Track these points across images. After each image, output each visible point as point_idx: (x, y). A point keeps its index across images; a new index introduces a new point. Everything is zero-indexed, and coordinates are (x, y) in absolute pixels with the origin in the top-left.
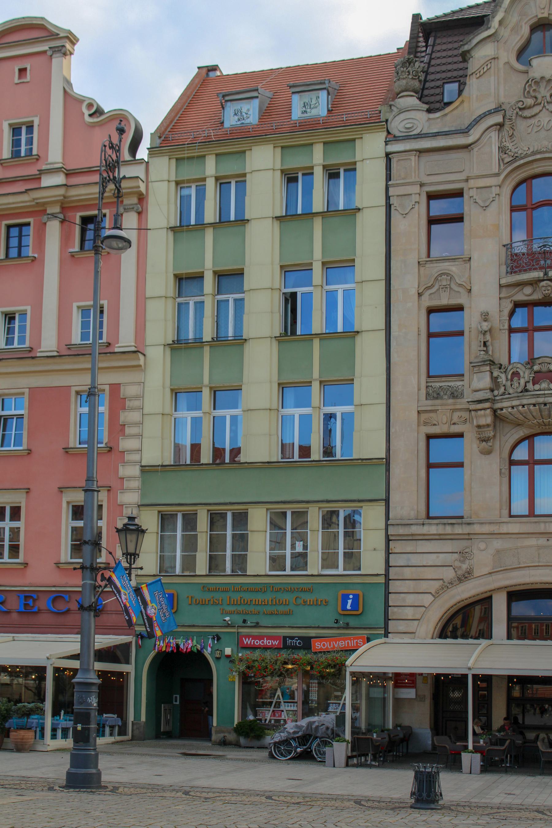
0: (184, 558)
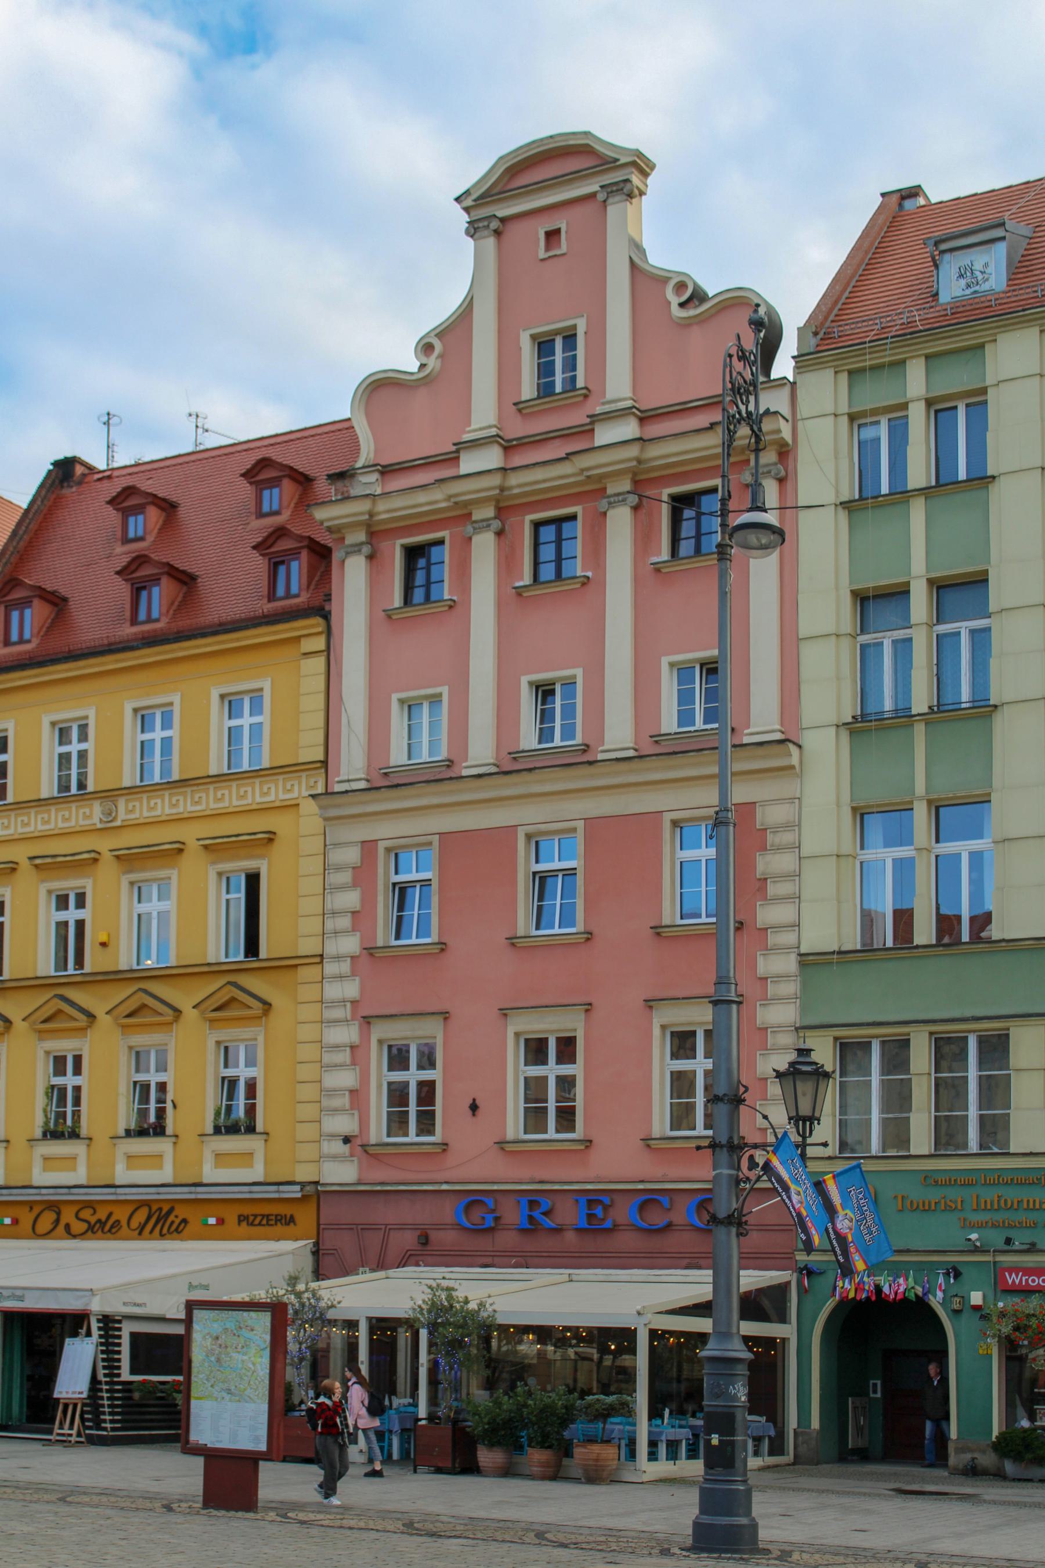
0: (885, 1123)
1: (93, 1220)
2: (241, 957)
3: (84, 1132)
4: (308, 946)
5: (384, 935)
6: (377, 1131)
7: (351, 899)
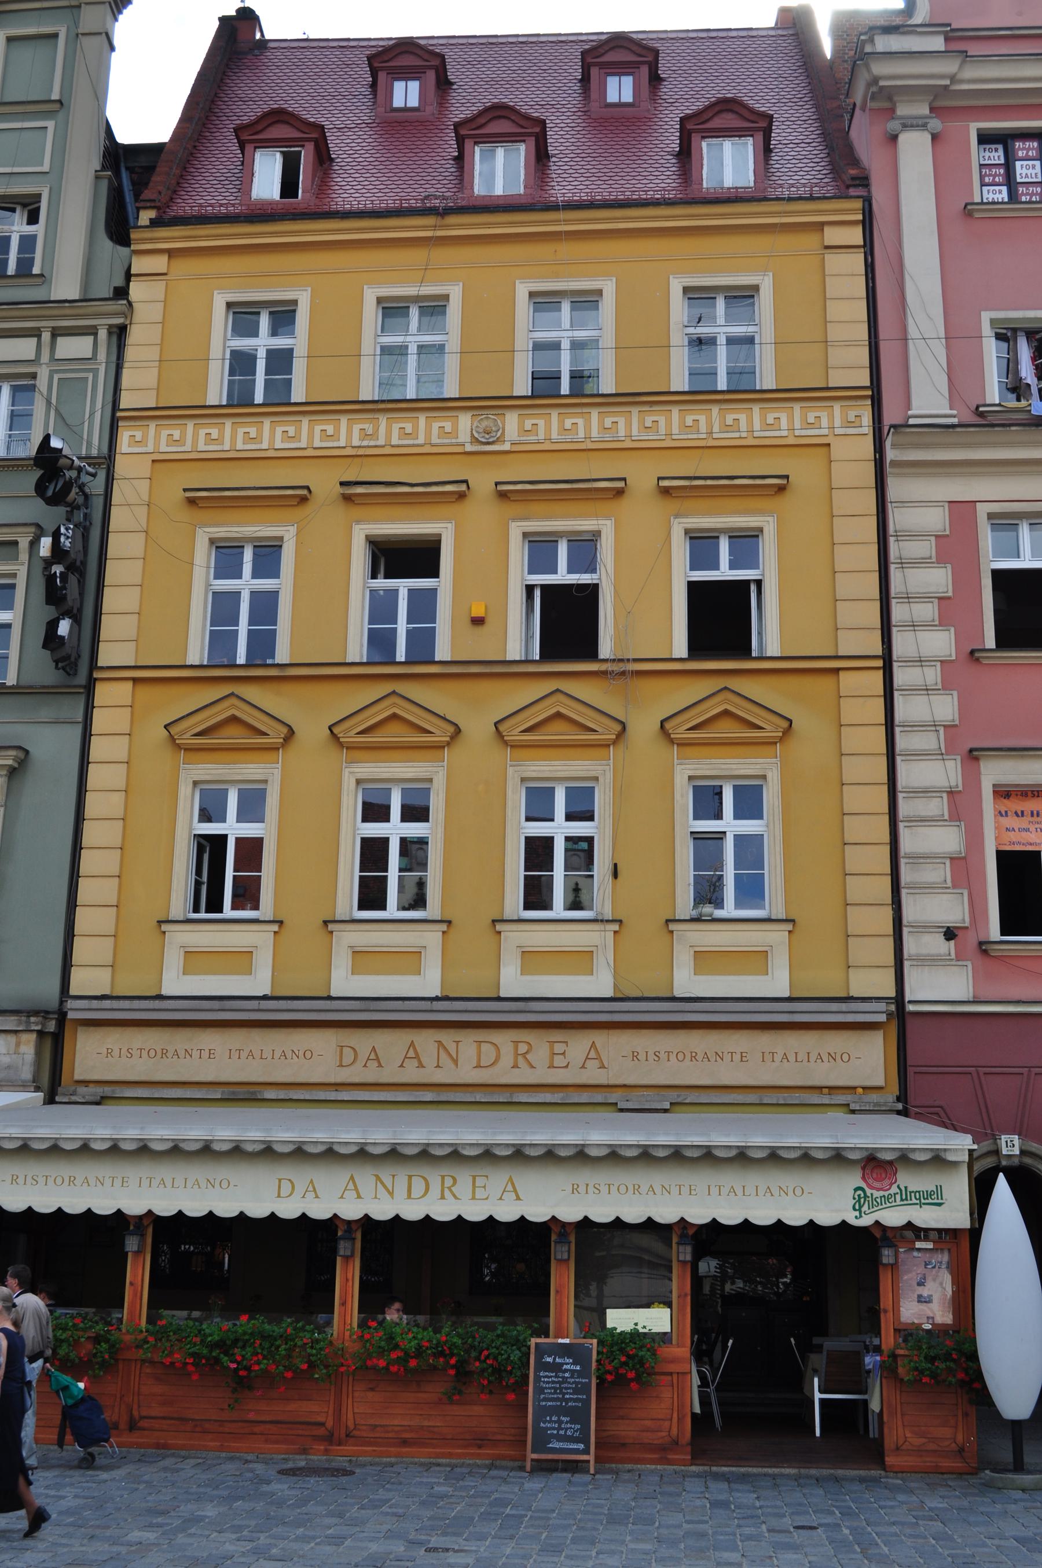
7: (939, 579)
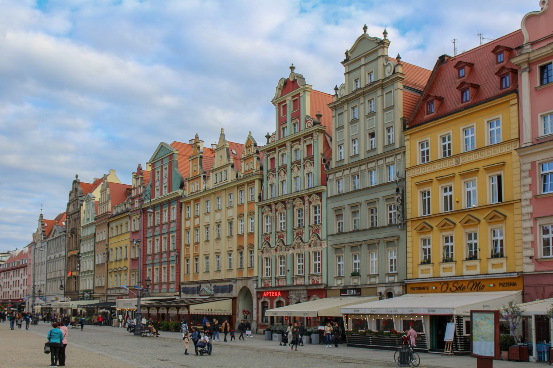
1: (458, 286)
2: (497, 202)
3: (454, 260)
4: (516, 197)
5: (540, 191)
6: (540, 254)
7: (529, 181)
